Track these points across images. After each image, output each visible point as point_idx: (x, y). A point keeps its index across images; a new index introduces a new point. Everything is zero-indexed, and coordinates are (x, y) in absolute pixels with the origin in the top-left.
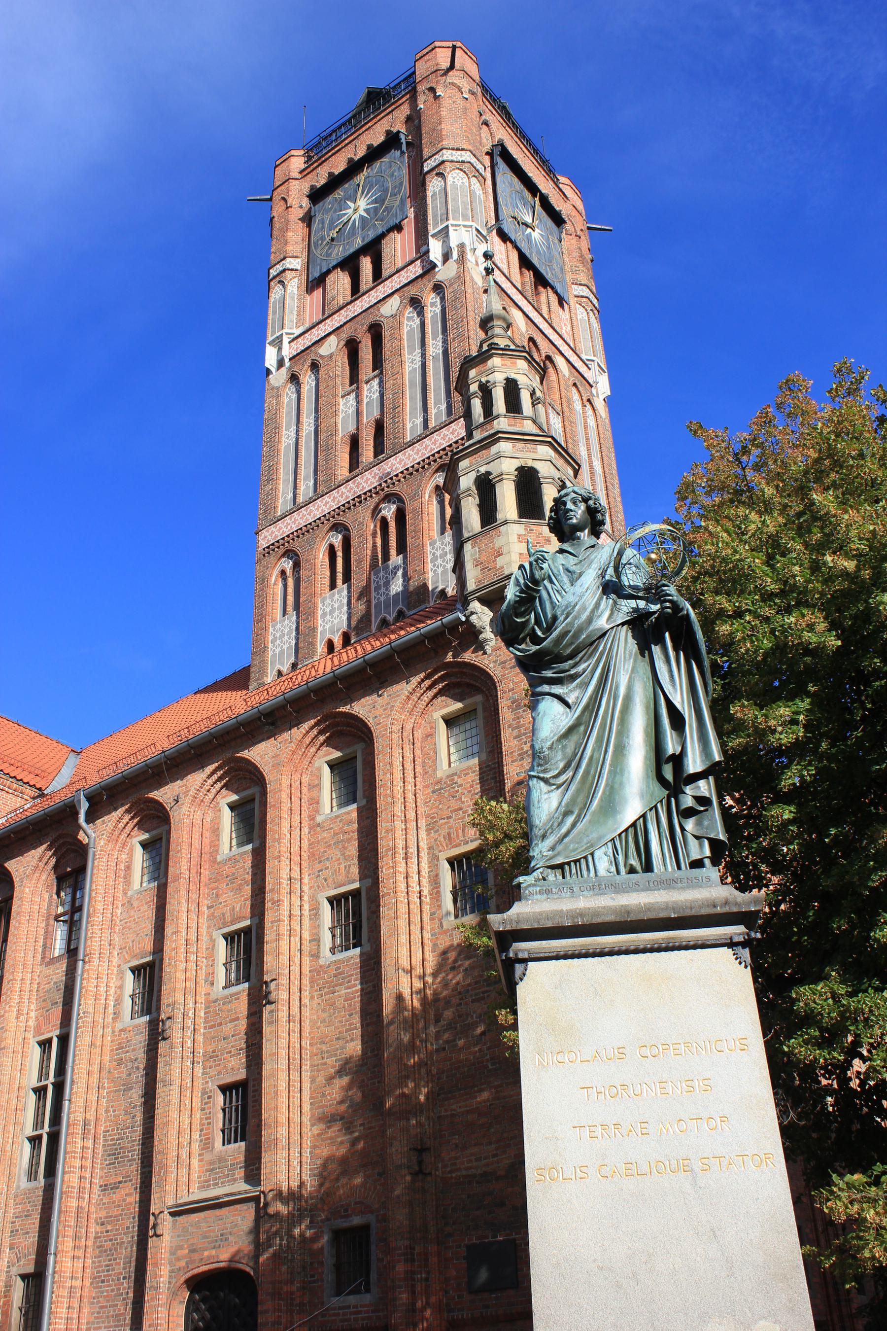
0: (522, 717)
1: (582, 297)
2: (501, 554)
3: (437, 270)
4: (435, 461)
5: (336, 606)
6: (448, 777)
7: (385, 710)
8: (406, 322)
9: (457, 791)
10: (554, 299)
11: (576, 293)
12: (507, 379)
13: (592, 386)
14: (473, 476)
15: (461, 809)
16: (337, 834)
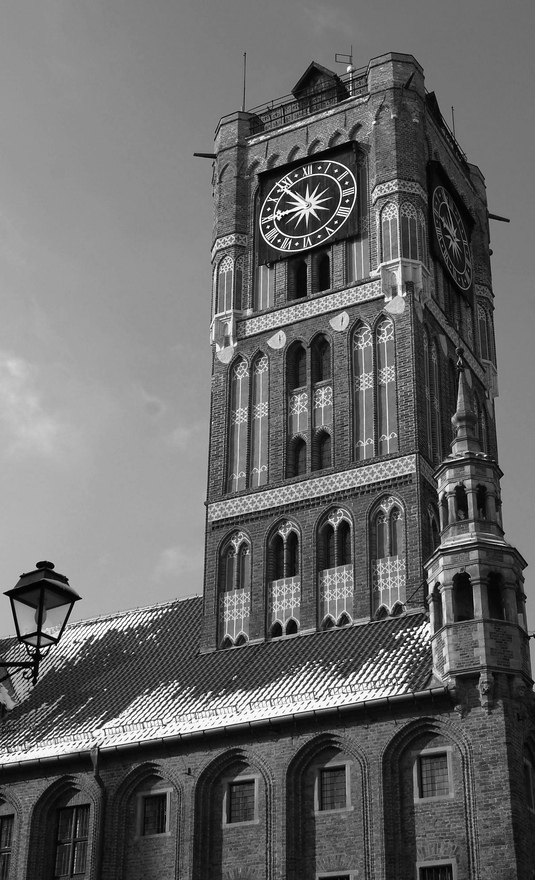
0: (488, 777)
1: (483, 297)
2: (477, 647)
3: (386, 300)
4: (379, 489)
5: (284, 594)
6: (423, 804)
7: (375, 743)
8: (354, 341)
9: (432, 817)
10: (463, 304)
11: (478, 293)
12: (479, 486)
13: (485, 389)
14: (453, 573)
15: (434, 832)
16: (330, 829)
